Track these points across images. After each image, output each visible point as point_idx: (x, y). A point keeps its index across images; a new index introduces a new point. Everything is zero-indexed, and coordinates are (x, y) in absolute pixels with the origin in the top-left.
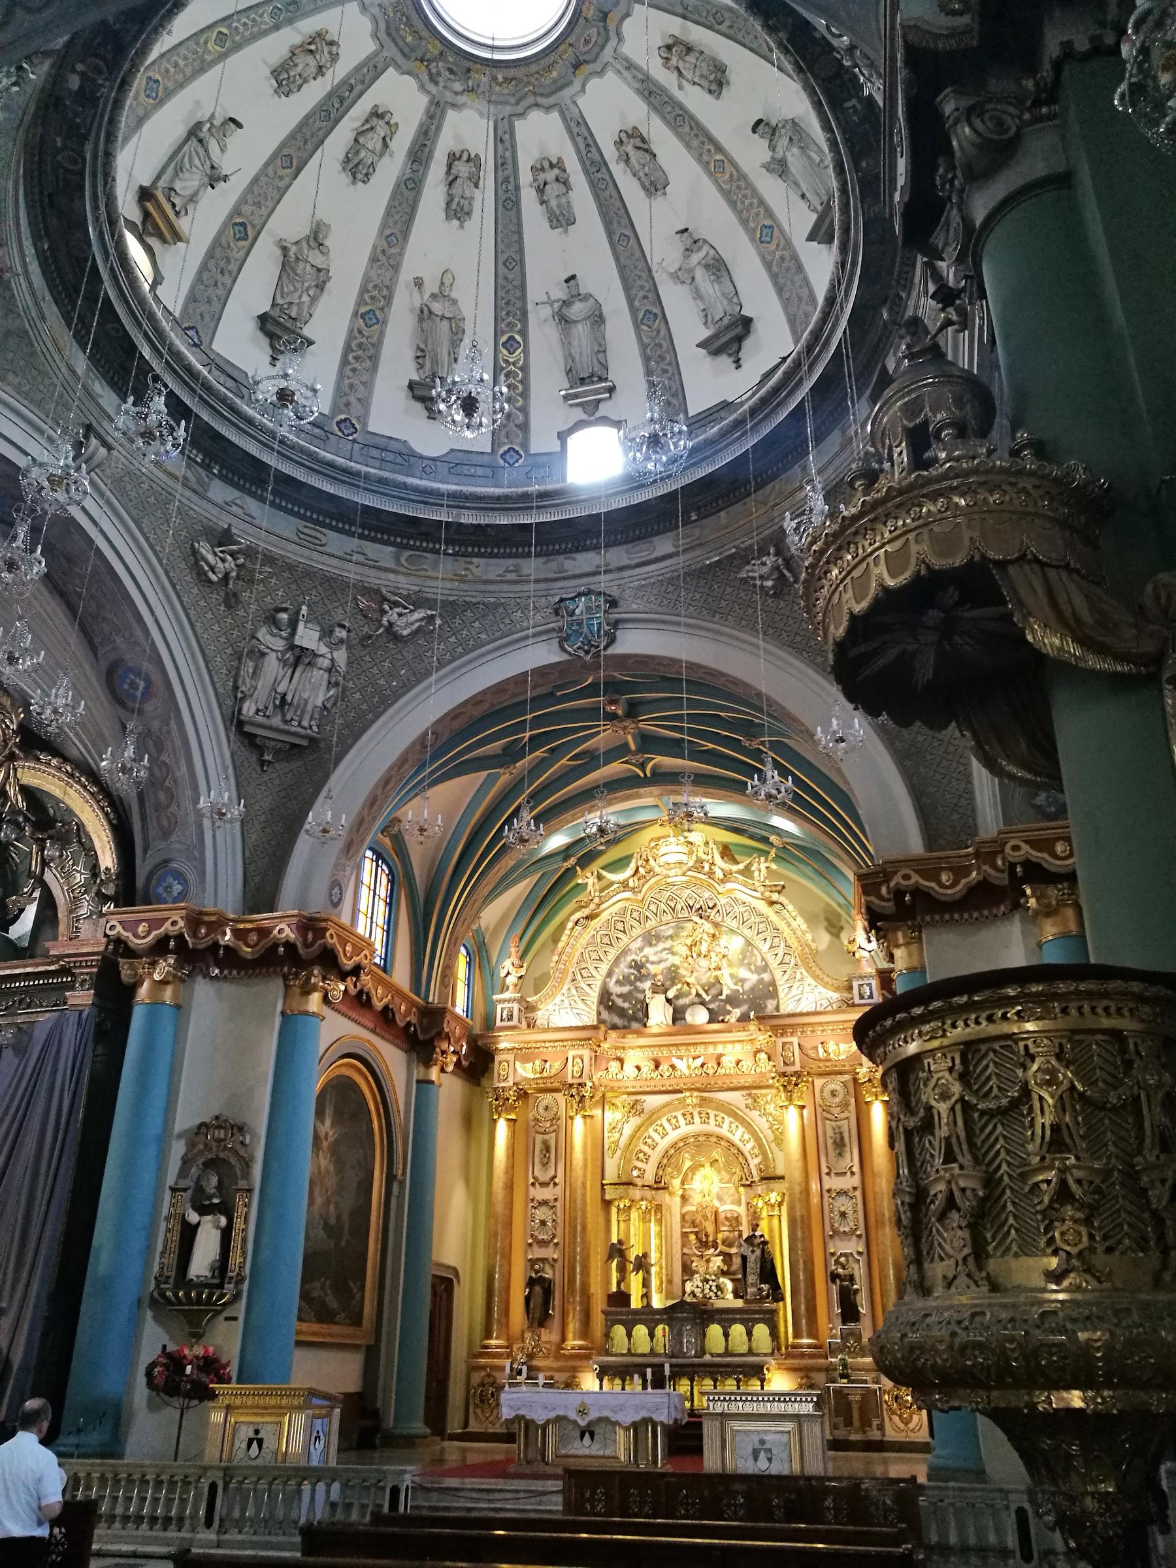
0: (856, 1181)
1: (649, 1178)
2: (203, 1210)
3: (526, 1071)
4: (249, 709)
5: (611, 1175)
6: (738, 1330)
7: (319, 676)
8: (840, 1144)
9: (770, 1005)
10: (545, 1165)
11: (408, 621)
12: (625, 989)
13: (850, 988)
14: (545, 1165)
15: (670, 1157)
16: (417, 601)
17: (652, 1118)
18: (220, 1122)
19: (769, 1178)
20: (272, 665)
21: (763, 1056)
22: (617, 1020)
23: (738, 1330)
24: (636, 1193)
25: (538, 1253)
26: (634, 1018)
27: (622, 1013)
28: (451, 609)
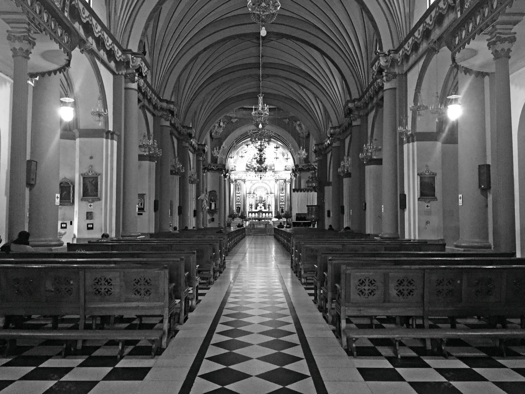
0: (284, 195)
1: (252, 193)
2: (212, 202)
3: (237, 177)
4: (213, 134)
5: (248, 192)
6: (267, 214)
7: (222, 129)
8: (282, 189)
9: (273, 168)
10: (238, 191)
11: (234, 121)
12: (250, 163)
13: (286, 167)
14: (238, 191)
15: (256, 189)
16: (236, 118)
17: (254, 184)
18: (213, 191)
19: (271, 193)
20: (216, 128)
21: (272, 176)
22: (248, 168)
23: (267, 214)
24: (251, 195)
25: (237, 203)
26: (251, 168)
27: (249, 167)
28: (240, 119)
